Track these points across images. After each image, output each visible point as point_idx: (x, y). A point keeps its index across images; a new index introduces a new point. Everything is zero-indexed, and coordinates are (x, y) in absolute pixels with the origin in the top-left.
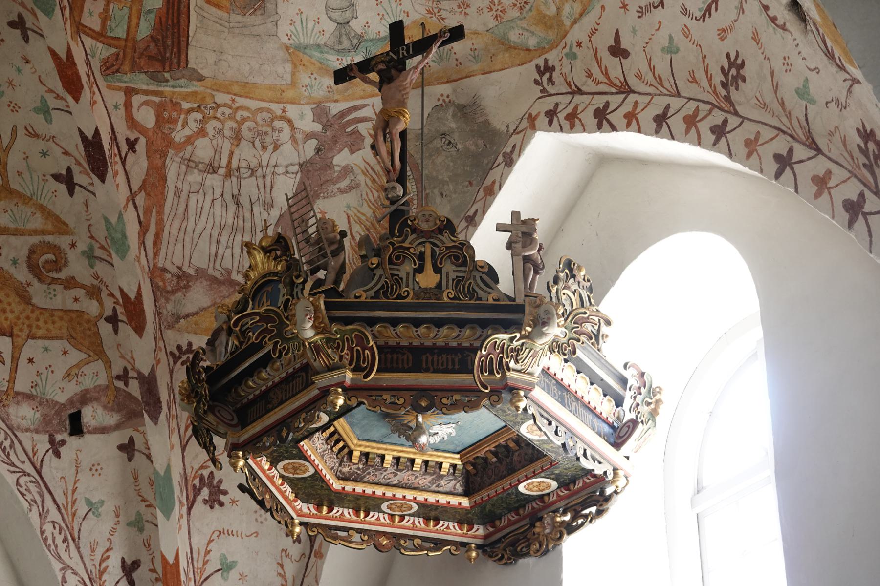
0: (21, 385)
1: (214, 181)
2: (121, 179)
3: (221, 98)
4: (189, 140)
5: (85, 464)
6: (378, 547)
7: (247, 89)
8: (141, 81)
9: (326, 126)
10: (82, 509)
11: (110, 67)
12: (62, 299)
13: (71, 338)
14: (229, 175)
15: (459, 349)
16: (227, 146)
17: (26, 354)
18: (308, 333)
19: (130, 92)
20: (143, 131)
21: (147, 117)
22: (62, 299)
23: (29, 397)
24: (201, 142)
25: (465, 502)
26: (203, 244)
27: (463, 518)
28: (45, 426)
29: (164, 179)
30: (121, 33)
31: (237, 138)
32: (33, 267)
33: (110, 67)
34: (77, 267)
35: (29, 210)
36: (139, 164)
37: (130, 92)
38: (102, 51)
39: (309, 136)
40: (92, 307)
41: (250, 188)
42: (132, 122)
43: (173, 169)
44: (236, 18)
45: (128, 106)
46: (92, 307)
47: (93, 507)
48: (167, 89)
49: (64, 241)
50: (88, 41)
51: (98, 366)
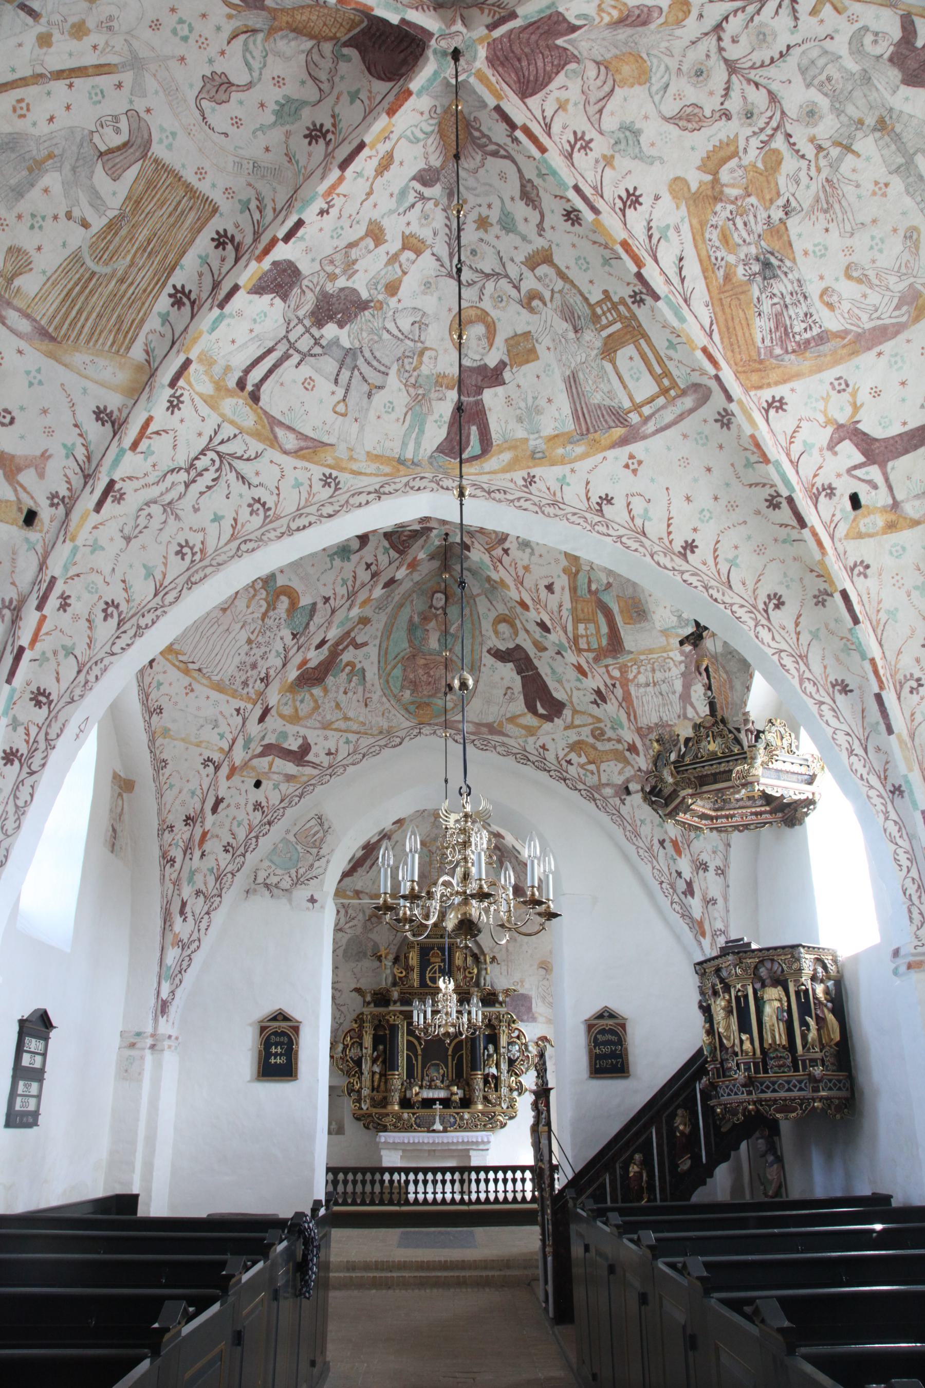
0: (604, 781)
1: (650, 689)
2: (614, 700)
3: (642, 657)
4: (635, 677)
5: (635, 805)
6: (740, 831)
7: (651, 651)
8: (609, 661)
9: (686, 657)
10: (639, 823)
11: (597, 660)
12: (608, 746)
13: (616, 760)
14: (655, 685)
15: (725, 772)
16: (650, 675)
17: (602, 769)
18: (670, 780)
19: (606, 666)
20: (616, 679)
21: (616, 673)
22: (608, 746)
23: (608, 785)
24: (640, 676)
25: (768, 808)
26: (654, 713)
27: (770, 813)
28: (617, 794)
29: (630, 694)
30: (596, 646)
31: (653, 670)
32: (594, 737)
33: (597, 660)
34: (610, 733)
35: (586, 717)
36: (619, 692)
37: (606, 666)
38: (591, 656)
39: (681, 662)
40: (620, 747)
41: (664, 688)
42: (611, 677)
43: (632, 689)
44: (638, 626)
45: (608, 671)
46: (620, 747)
47: (642, 822)
48: (620, 661)
49: (601, 725)
50: (585, 654)
51: (629, 767)
